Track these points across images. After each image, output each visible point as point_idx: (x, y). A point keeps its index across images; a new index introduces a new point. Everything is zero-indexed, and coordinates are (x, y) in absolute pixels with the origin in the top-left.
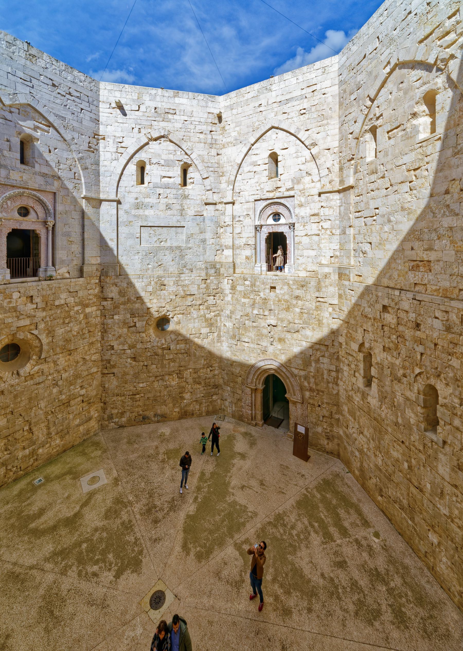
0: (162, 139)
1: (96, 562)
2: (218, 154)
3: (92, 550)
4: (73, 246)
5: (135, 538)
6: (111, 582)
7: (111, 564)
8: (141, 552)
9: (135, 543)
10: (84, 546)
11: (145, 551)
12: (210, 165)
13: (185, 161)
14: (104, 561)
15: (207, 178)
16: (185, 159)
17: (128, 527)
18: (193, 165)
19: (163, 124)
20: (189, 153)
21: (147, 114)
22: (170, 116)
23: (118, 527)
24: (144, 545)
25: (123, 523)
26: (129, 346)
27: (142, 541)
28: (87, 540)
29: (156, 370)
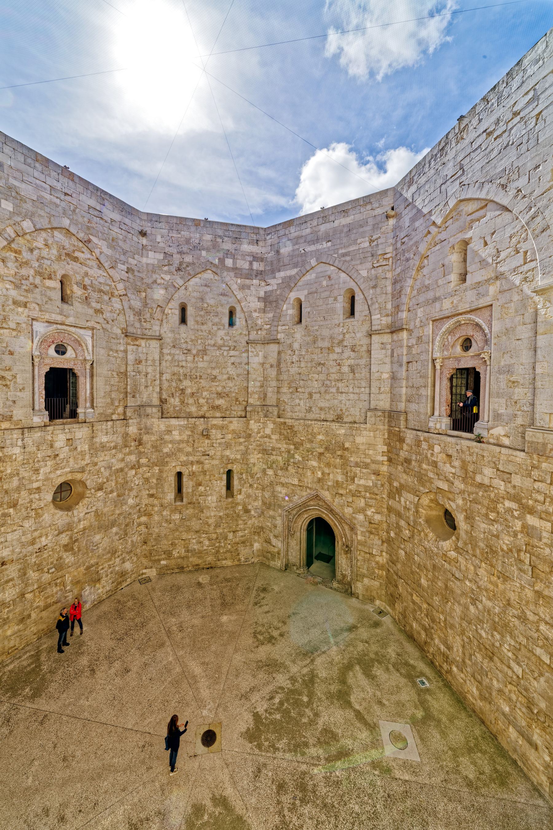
1: (281, 703)
3: (297, 703)
5: (278, 749)
6: (255, 708)
7: (270, 714)
8: (259, 747)
9: (273, 746)
10: (305, 699)
11: (257, 751)
14: (277, 709)
17: (298, 747)
23: (305, 737)
24: (263, 754)
25: (306, 745)
27: (269, 755)
28: (310, 703)
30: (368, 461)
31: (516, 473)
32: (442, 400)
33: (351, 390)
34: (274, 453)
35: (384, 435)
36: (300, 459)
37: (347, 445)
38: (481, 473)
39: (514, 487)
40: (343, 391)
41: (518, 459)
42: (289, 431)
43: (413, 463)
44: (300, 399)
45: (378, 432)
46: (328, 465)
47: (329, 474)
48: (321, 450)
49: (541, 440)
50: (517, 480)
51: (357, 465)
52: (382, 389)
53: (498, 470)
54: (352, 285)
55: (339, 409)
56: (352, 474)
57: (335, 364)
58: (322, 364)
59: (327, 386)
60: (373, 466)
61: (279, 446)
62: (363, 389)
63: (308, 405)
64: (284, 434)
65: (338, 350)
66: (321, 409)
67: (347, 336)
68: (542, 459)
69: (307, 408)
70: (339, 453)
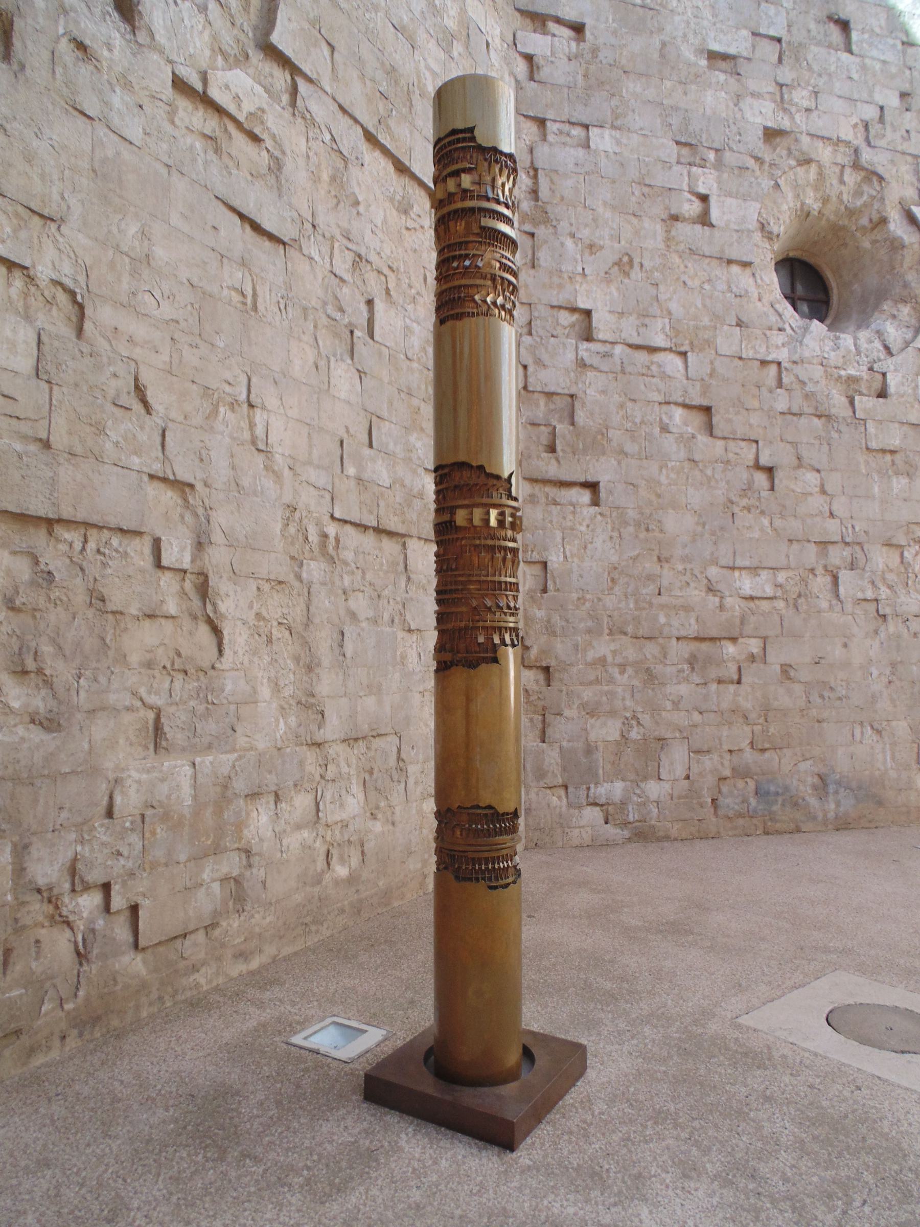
29: (817, 502)
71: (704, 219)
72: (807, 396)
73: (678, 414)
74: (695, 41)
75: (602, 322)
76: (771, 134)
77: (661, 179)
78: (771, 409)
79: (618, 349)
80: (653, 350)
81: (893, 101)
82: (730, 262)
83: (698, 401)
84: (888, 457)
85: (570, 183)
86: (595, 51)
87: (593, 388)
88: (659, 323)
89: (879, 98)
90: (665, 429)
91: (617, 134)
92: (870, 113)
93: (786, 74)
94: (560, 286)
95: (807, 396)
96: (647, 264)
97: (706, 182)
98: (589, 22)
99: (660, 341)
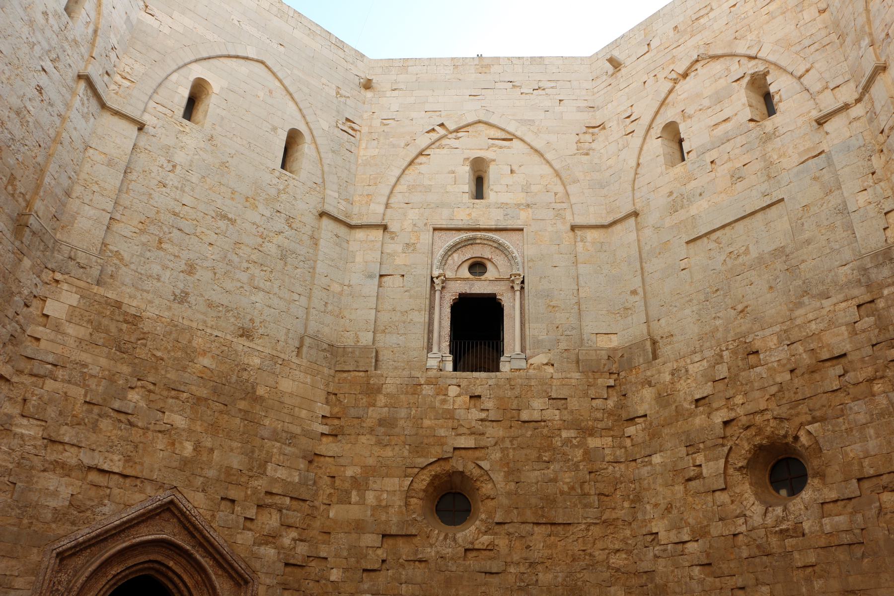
0: (698, 66)
2: (822, 11)
4: (558, 315)
12: (807, 42)
13: (752, 71)
15: (807, 71)
16: (752, 67)
18: (772, 69)
19: (691, 43)
20: (752, 53)
21: (662, 48)
22: (702, 21)
26: (693, 531)
30: (298, 430)
31: (571, 397)
32: (443, 333)
33: (276, 290)
34: (60, 373)
35: (327, 385)
36: (142, 404)
37: (261, 391)
38: (528, 407)
39: (572, 412)
40: (261, 285)
41: (573, 381)
42: (124, 326)
43: (401, 423)
44: (165, 267)
45: (318, 378)
46: (214, 428)
47: (212, 450)
48: (204, 392)
49: (594, 358)
50: (573, 404)
51: (275, 436)
52: (330, 308)
53: (550, 398)
54: (302, 128)
55: (249, 317)
56: (263, 455)
57: (254, 231)
58: (230, 220)
59: (230, 263)
60: (304, 442)
61: (85, 357)
62: (296, 297)
63: (181, 286)
64: (107, 332)
65: (261, 208)
66: (210, 305)
67: (283, 197)
68: (597, 375)
69: (177, 292)
70: (242, 405)
71: (699, 476)
72: (758, 547)
73: (697, 570)
74: (689, 398)
75: (662, 536)
76: (726, 423)
77: (681, 465)
78: (740, 557)
79: (669, 547)
80: (684, 543)
81: (788, 376)
82: (714, 491)
83: (706, 562)
84: (810, 569)
85: (646, 482)
86: (651, 424)
87: (662, 566)
88: (685, 530)
89: (779, 380)
90: (691, 578)
91: (662, 454)
92: (774, 389)
93: (730, 393)
94: (646, 526)
95: (758, 547)
96: (678, 505)
97: (700, 458)
98: (648, 413)
99: (686, 538)
